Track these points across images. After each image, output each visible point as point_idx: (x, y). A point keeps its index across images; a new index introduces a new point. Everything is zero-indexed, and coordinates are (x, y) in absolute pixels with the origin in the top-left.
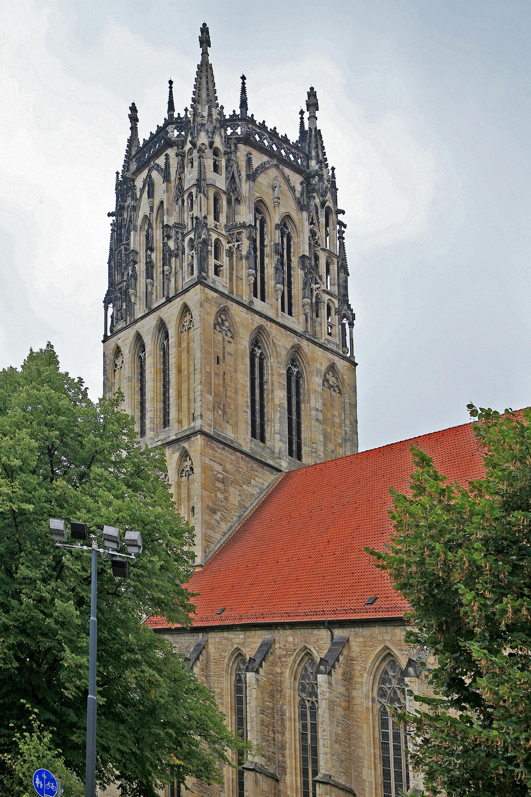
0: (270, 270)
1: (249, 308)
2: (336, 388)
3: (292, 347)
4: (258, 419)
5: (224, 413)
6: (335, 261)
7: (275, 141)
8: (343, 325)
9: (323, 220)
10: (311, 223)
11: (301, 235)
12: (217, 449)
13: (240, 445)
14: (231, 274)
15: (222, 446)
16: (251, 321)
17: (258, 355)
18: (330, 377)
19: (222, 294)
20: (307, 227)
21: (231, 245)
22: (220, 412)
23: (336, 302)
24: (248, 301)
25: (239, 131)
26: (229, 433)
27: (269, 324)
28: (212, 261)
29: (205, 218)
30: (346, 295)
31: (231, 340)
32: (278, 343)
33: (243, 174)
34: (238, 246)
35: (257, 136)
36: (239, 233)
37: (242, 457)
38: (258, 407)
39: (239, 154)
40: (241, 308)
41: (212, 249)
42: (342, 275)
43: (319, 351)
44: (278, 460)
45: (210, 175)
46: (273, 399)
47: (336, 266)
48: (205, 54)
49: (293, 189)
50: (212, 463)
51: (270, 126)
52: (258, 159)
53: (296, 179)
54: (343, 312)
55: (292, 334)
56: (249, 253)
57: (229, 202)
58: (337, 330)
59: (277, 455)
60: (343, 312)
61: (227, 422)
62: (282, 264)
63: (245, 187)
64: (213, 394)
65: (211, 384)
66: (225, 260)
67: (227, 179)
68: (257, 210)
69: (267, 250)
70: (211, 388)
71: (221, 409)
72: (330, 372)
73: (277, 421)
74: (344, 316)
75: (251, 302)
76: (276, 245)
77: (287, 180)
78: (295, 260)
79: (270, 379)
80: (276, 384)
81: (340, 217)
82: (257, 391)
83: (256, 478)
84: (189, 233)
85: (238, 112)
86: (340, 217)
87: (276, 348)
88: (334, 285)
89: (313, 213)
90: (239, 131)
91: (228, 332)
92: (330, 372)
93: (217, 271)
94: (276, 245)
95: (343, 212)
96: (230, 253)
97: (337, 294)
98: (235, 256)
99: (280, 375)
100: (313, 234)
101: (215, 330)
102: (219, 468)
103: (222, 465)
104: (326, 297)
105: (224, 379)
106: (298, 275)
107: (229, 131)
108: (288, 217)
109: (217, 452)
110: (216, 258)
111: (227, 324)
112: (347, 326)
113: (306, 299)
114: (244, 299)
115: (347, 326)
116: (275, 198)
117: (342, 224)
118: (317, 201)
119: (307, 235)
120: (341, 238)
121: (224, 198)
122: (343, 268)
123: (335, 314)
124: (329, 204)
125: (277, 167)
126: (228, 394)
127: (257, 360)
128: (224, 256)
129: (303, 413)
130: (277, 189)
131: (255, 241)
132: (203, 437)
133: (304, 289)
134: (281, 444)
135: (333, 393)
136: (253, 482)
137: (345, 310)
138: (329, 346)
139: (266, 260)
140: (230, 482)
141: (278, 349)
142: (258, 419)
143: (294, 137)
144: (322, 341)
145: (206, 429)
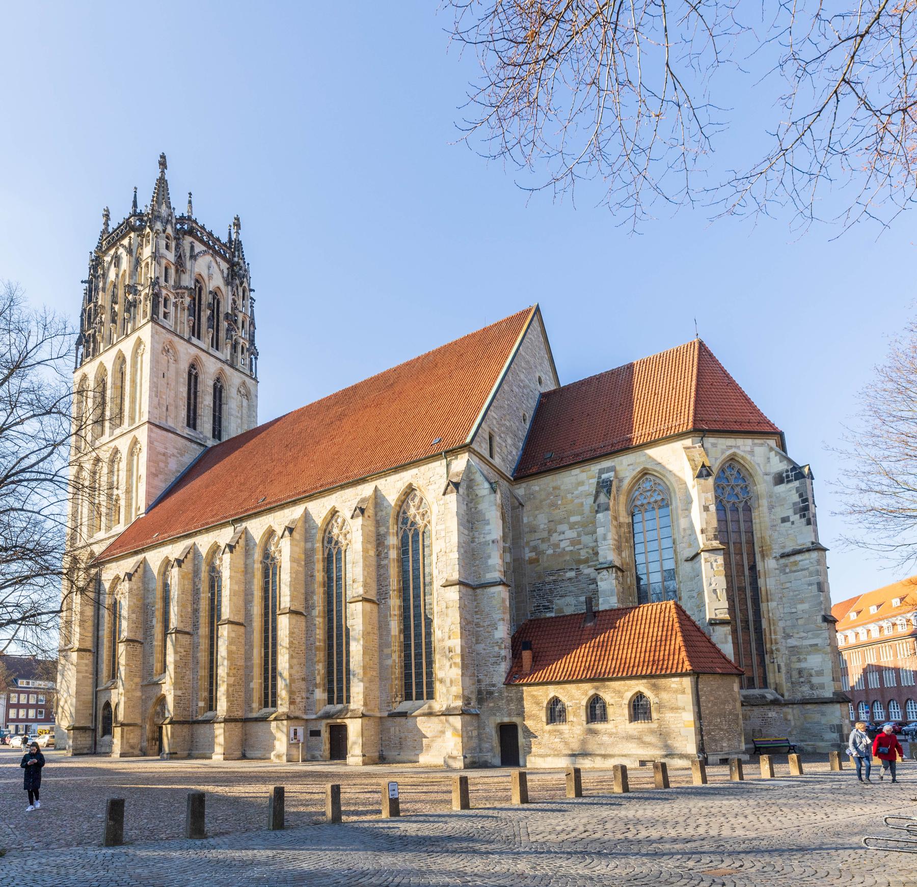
0: (204, 319)
1: (189, 341)
4: (192, 415)
7: (211, 238)
8: (251, 359)
9: (241, 294)
10: (234, 295)
14: (176, 317)
20: (230, 297)
25: (186, 227)
26: (171, 423)
28: (162, 309)
29: (158, 278)
33: (188, 255)
35: (198, 233)
38: (192, 407)
39: (185, 242)
40: (182, 341)
41: (162, 300)
42: (252, 329)
43: (236, 373)
45: (163, 250)
48: (163, 172)
51: (208, 229)
52: (199, 247)
53: (224, 266)
56: (190, 305)
57: (177, 271)
62: (213, 316)
63: (188, 264)
66: (171, 309)
67: (176, 256)
68: (197, 281)
69: (203, 307)
75: (190, 338)
76: (209, 304)
77: (219, 266)
78: (222, 316)
81: (252, 293)
82: (192, 396)
85: (186, 215)
86: (252, 294)
89: (235, 289)
90: (186, 227)
93: (166, 315)
94: (209, 304)
95: (254, 291)
96: (175, 304)
100: (234, 302)
106: (224, 325)
107: (178, 226)
110: (165, 306)
117: (251, 298)
118: (238, 282)
119: (230, 301)
120: (252, 306)
121: (173, 267)
125: (212, 256)
127: (193, 377)
131: (194, 299)
139: (202, 314)
142: (192, 415)
143: (224, 239)
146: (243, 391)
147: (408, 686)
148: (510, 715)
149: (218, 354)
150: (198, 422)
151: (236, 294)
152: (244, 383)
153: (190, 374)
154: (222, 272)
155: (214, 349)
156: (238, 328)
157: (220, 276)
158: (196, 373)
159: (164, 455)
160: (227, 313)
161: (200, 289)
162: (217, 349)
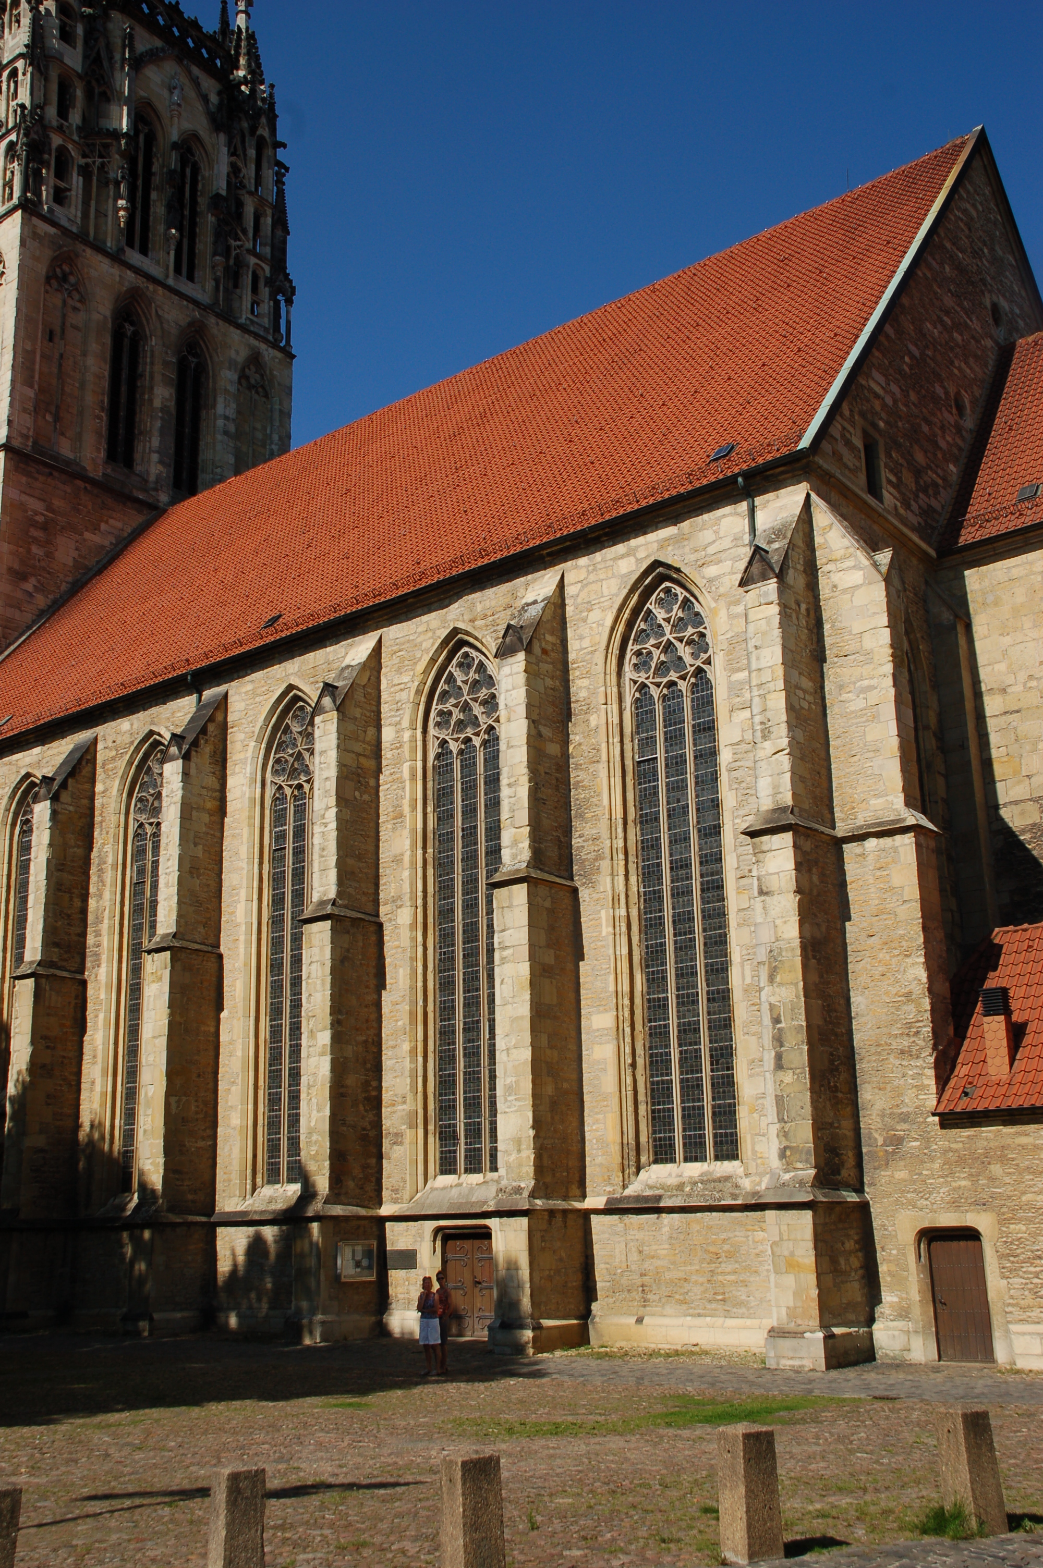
1: (116, 258)
2: (260, 390)
3: (190, 324)
5: (57, 418)
6: (269, 212)
8: (277, 304)
9: (252, 153)
11: (216, 167)
12: (37, 475)
13: (84, 467)
15: (47, 470)
16: (117, 279)
17: (129, 333)
18: (251, 372)
19: (65, 231)
21: (89, 160)
22: (49, 418)
23: (267, 269)
24: (114, 248)
26: (65, 449)
27: (151, 287)
30: (284, 261)
31: (78, 305)
32: (166, 316)
34: (103, 165)
36: (106, 146)
37: (86, 488)
40: (100, 257)
42: (279, 233)
44: (153, 493)
46: (151, 401)
47: (269, 220)
49: (205, 99)
50: (24, 498)
54: (278, 283)
55: (191, 306)
58: (266, 307)
59: (152, 485)
60: (278, 283)
61: (63, 434)
64: (36, 387)
65: (33, 370)
69: (156, 180)
70: (33, 377)
71: (51, 413)
72: (252, 367)
73: (156, 433)
74: (280, 290)
75: (121, 250)
77: (196, 83)
78: (203, 202)
79: (148, 370)
80: (158, 378)
82: (124, 388)
83: (111, 521)
84: (8, 132)
86: (281, 154)
87: (161, 323)
88: (265, 245)
89: (237, 141)
91: (74, 293)
92: (252, 367)
94: (172, 172)
95: (284, 146)
96: (85, 172)
97: (269, 256)
98: (95, 178)
99: (166, 364)
101: (48, 288)
102: (38, 506)
103: (44, 501)
104: (253, 260)
105: (60, 365)
108: (195, 136)
109: (37, 479)
111: (72, 279)
112: (283, 304)
113: (217, 258)
114: (109, 244)
115: (283, 304)
116: (173, 104)
117: (280, 164)
118: (245, 125)
120: (279, 182)
122: (281, 222)
123: (265, 286)
124: (264, 132)
126: (66, 389)
127: (126, 342)
128: (75, 175)
129: (203, 425)
130: (176, 92)
132: (10, 455)
133: (215, 243)
134: (160, 467)
135: (256, 396)
136: (103, 526)
137: (281, 281)
138: (252, 329)
139: (154, 195)
140: (58, 527)
141: (166, 326)
144: (242, 321)
145: (16, 443)
146: (255, 378)
147: (661, 1120)
148: (955, 1204)
149: (187, 288)
150: (139, 448)
151: (240, 152)
152: (255, 359)
153: (118, 336)
154: (205, 99)
155: (184, 279)
156: (245, 232)
157: (199, 106)
158: (135, 333)
159: (45, 527)
160: (218, 195)
161: (151, 139)
162: (191, 278)
